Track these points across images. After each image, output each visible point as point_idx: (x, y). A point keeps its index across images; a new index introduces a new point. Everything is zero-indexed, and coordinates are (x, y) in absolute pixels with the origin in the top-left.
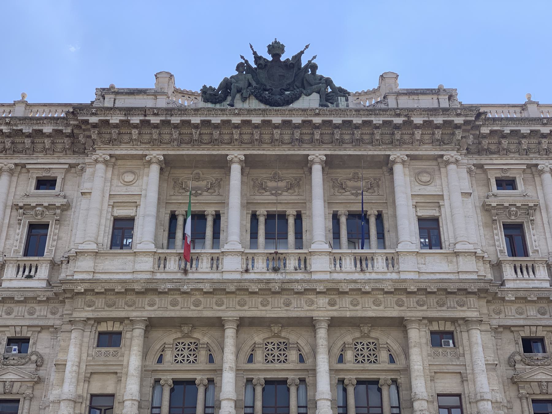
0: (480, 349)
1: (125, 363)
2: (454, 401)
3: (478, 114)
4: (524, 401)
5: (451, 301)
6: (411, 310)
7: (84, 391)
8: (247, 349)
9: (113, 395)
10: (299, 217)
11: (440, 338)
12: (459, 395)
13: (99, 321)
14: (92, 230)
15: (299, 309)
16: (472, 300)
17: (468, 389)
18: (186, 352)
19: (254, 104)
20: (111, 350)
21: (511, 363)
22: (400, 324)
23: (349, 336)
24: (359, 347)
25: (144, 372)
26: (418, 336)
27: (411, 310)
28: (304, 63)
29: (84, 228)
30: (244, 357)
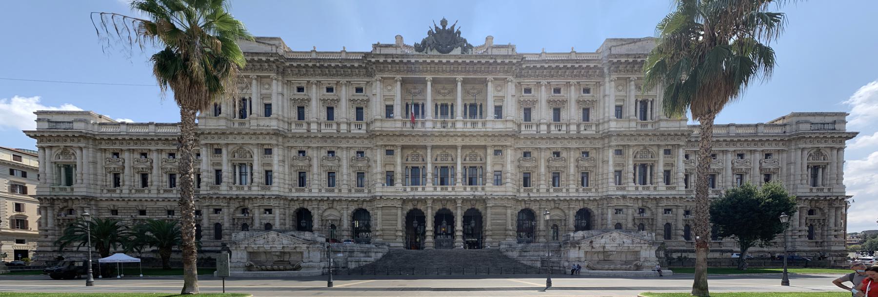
0: (510, 156)
3: (522, 57)
5: (502, 139)
6: (489, 142)
7: (384, 170)
8: (435, 156)
10: (452, 106)
11: (497, 152)
13: (386, 146)
14: (379, 110)
15: (452, 142)
16: (510, 139)
19: (435, 52)
21: (519, 161)
22: (485, 147)
23: (468, 152)
25: (402, 164)
26: (490, 151)
27: (489, 142)
28: (455, 31)
29: (376, 110)
30: (434, 159)
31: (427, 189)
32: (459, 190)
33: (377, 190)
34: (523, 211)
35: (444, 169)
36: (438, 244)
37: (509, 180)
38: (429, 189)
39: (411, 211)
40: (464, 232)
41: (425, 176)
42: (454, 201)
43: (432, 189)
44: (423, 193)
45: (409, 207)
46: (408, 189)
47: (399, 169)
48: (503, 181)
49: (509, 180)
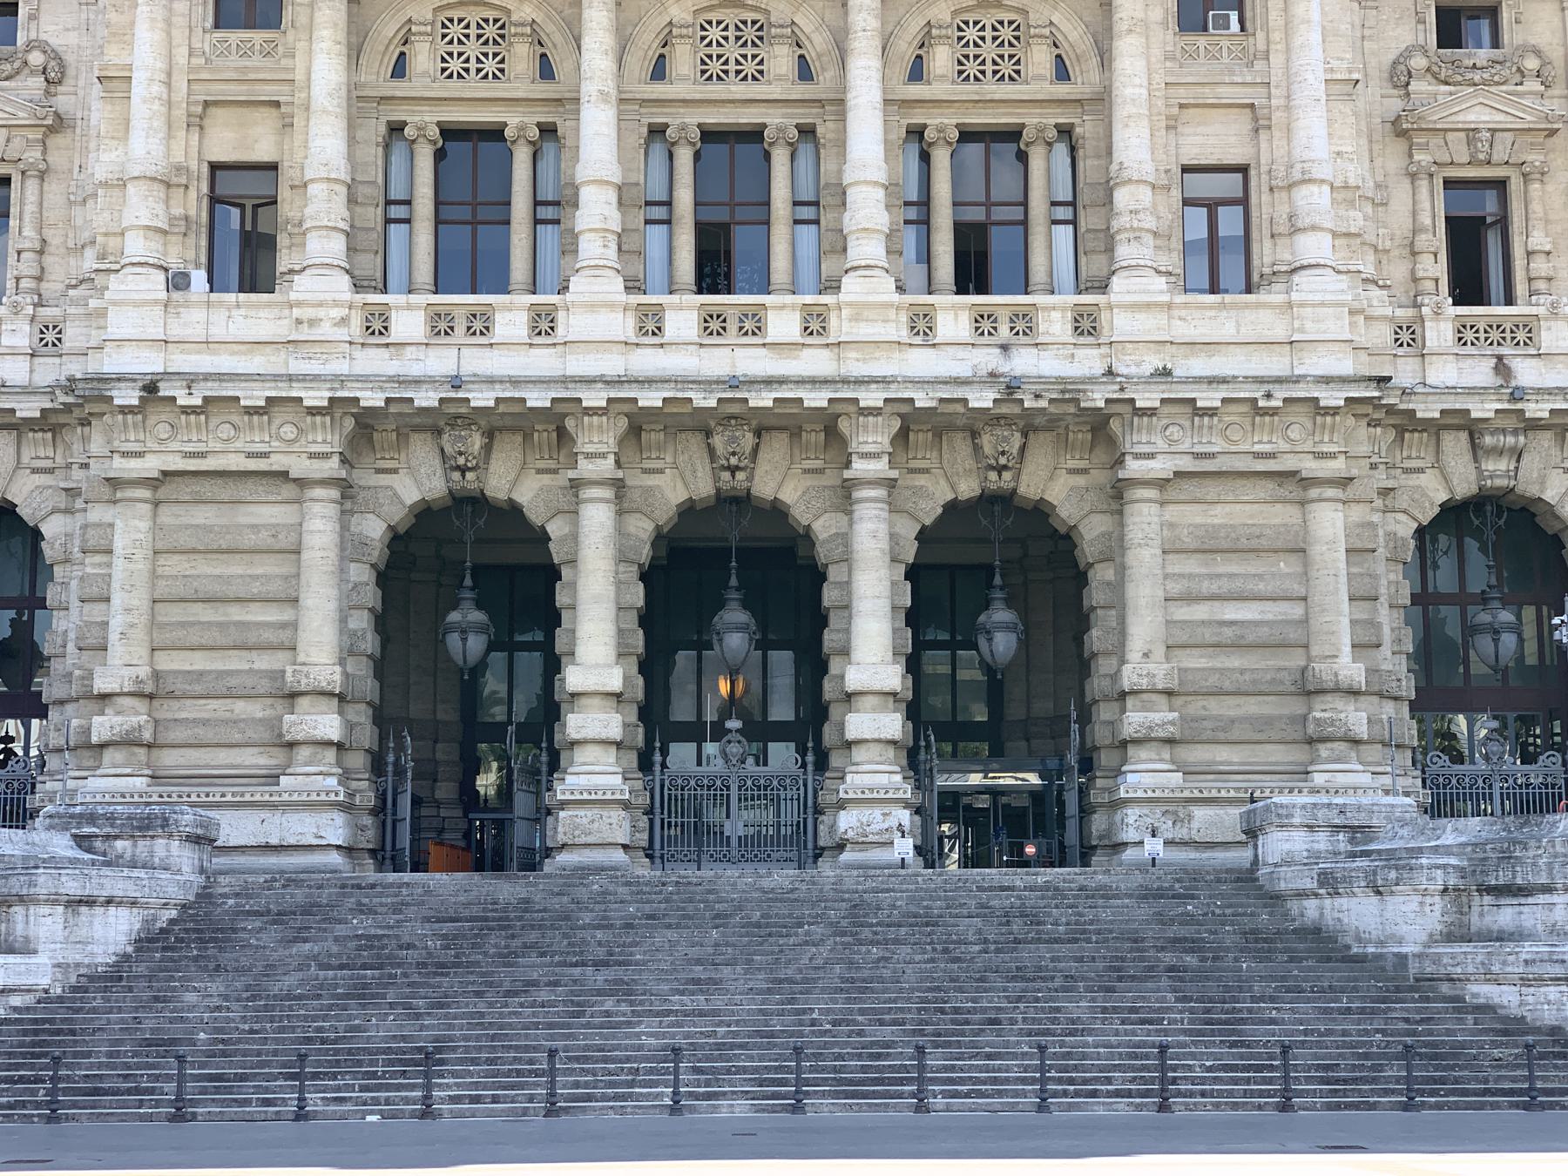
1: (299, 76)
2: (1228, 185)
4: (1423, 184)
7: (191, 153)
9: (273, 167)
12: (1243, 170)
17: (1269, 154)
18: (473, 49)
20: (258, 36)
21: (1399, 76)
24: (971, 34)
25: (358, 102)
30: (640, 63)
31: (571, 325)
32: (864, 329)
33: (120, 324)
34: (1457, 518)
35: (733, 148)
36: (675, 824)
37: (1314, 247)
38: (599, 326)
39: (425, 514)
40: (914, 712)
41: (554, 209)
42: (823, 431)
43: (623, 326)
44: (542, 362)
45: (414, 481)
46: (409, 321)
47: (321, 156)
48: (1265, 254)
49: (1314, 247)
